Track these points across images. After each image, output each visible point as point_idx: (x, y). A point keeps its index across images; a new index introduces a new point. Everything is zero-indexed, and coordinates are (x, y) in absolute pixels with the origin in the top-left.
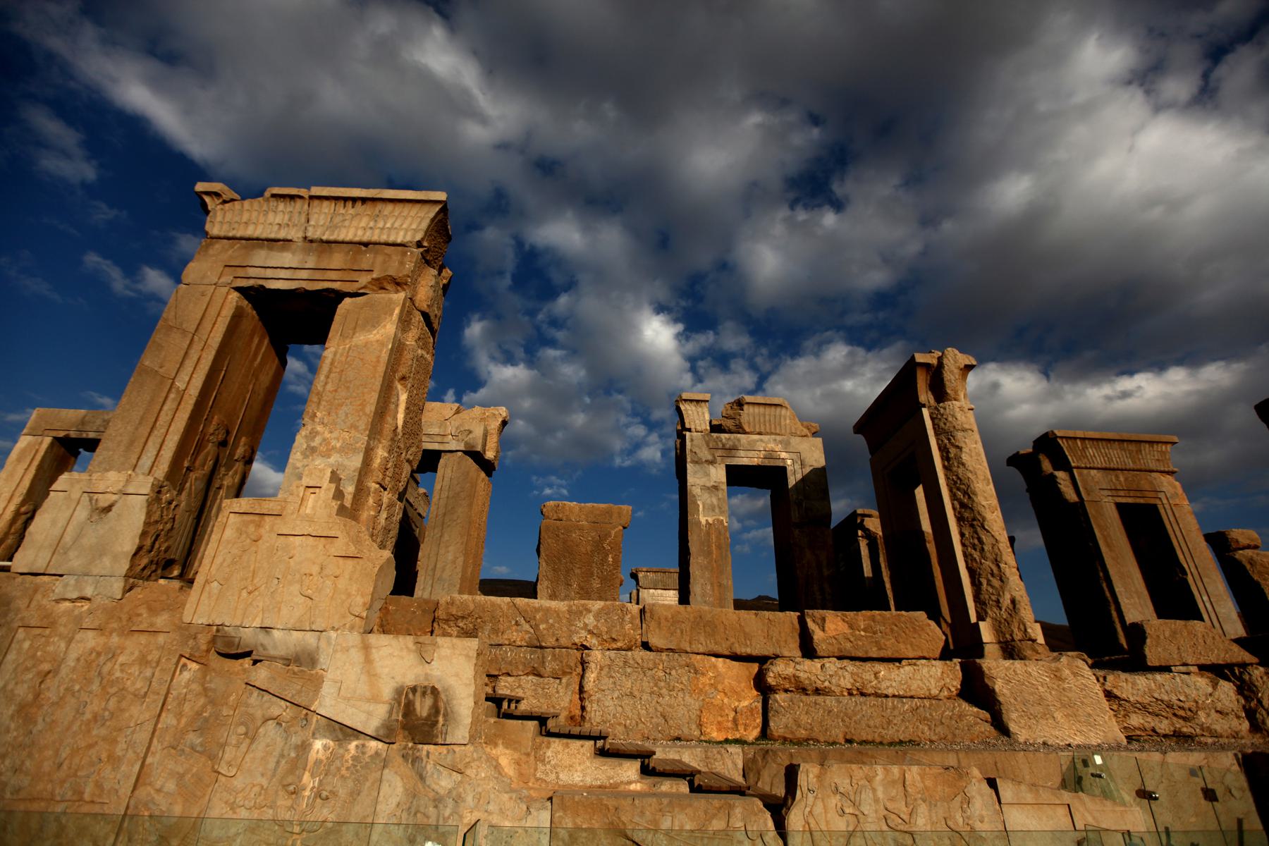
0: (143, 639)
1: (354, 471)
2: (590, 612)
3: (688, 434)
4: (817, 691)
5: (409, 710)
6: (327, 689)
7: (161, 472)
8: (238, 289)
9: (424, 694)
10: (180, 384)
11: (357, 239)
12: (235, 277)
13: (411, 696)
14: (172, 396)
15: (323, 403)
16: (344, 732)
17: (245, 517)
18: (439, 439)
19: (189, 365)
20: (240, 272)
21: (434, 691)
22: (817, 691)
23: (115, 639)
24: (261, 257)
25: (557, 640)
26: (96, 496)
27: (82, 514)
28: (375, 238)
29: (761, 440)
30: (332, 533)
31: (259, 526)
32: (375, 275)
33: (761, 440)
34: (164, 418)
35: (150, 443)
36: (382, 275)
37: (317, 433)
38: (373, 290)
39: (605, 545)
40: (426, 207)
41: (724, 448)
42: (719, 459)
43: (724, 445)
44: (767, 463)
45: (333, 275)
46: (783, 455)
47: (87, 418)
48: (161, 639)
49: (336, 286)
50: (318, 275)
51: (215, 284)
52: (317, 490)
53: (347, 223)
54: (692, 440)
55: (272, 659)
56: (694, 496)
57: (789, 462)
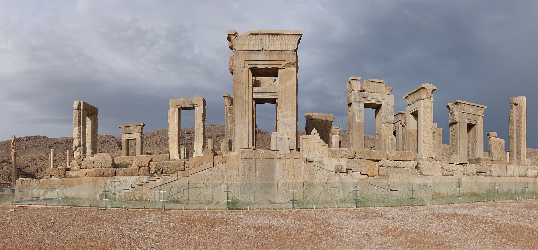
8: (250, 68)
20: (249, 63)
24: (253, 57)
45: (275, 62)
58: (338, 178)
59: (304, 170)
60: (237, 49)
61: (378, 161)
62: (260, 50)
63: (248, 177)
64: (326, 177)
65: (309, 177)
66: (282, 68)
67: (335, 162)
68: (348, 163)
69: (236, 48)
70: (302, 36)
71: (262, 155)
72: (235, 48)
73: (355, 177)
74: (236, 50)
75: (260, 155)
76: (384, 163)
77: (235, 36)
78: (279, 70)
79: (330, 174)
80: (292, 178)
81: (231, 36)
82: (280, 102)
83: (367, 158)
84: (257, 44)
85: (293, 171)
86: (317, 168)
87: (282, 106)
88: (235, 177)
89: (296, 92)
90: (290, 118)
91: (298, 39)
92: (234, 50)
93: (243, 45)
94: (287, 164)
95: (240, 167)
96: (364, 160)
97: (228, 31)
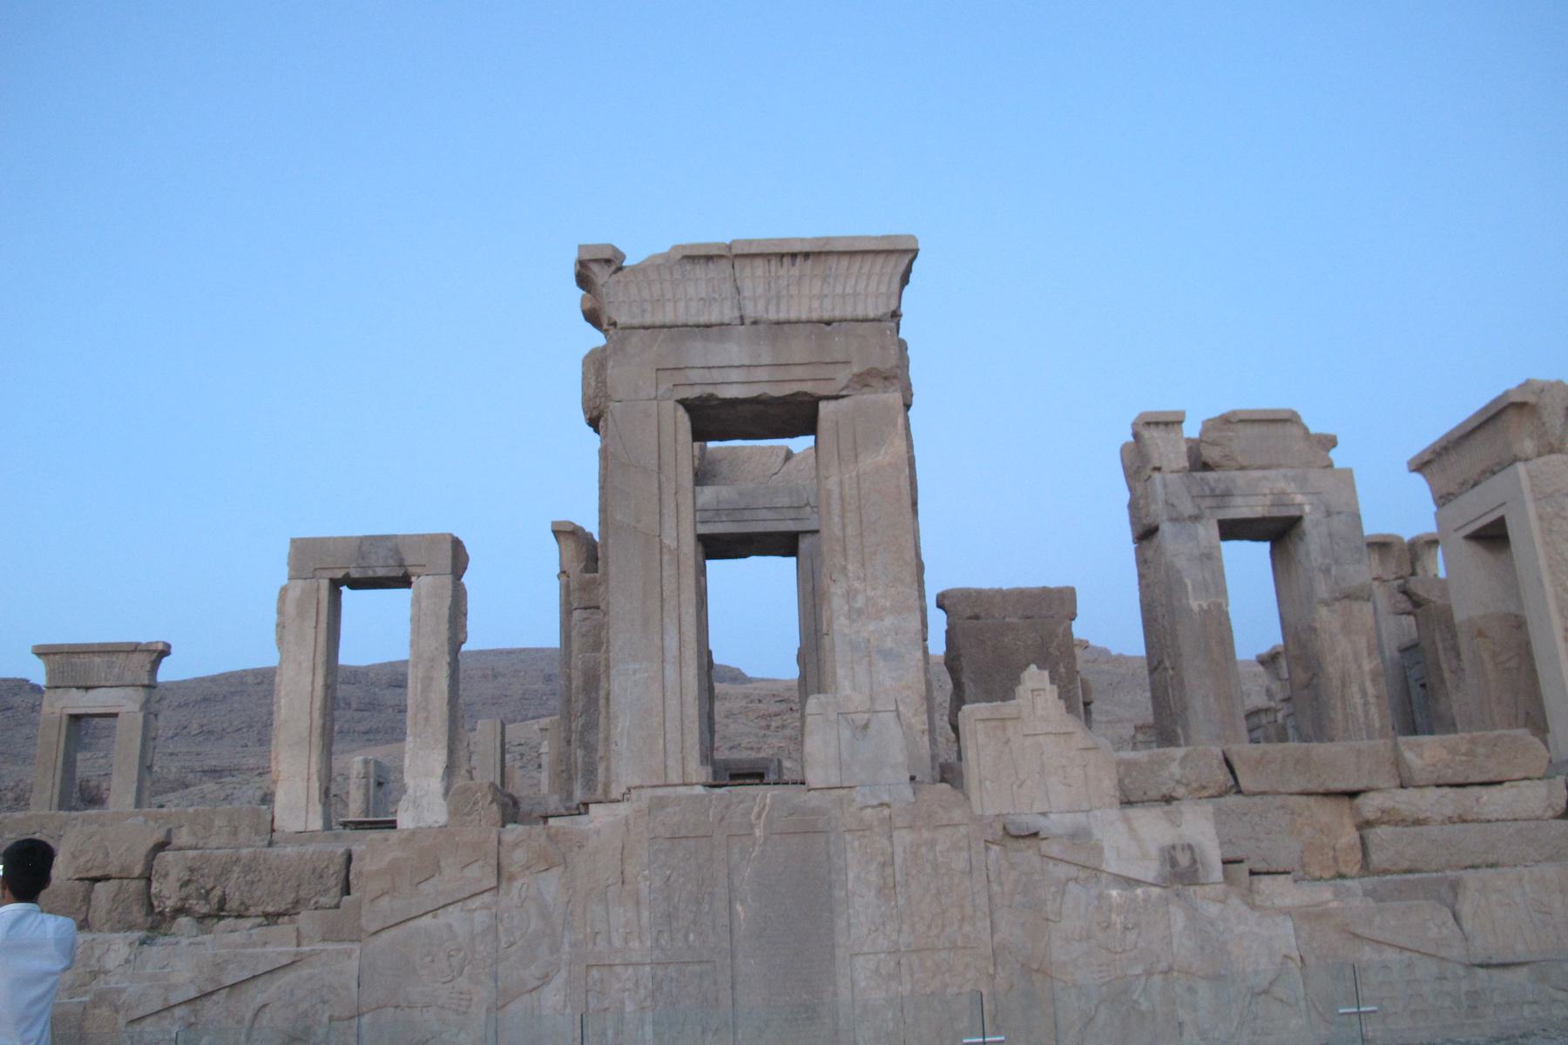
0: (948, 831)
1: (916, 634)
2: (1174, 760)
3: (1156, 475)
4: (1418, 822)
5: (1174, 863)
6: (1109, 854)
7: (692, 652)
8: (683, 402)
9: (1183, 849)
10: (669, 541)
11: (815, 316)
12: (674, 385)
13: (1172, 852)
14: (666, 558)
15: (850, 553)
16: (1130, 882)
17: (988, 723)
18: (792, 513)
19: (669, 511)
20: (679, 377)
21: (1190, 847)
22: (1418, 822)
23: (926, 834)
24: (697, 352)
25: (1145, 793)
26: (849, 717)
27: (846, 734)
28: (838, 314)
29: (1266, 478)
30: (1070, 729)
31: (1004, 729)
32: (856, 369)
33: (1266, 478)
34: (669, 588)
35: (667, 620)
36: (865, 369)
37: (857, 591)
38: (855, 389)
39: (1051, 650)
40: (893, 259)
41: (1213, 495)
42: (1208, 512)
43: (1212, 490)
44: (1276, 512)
45: (799, 372)
46: (1299, 498)
47: (364, 548)
48: (963, 830)
49: (808, 387)
50: (780, 374)
51: (655, 399)
52: (1041, 692)
53: (794, 290)
54: (1165, 486)
55: (1061, 837)
56: (1179, 572)
57: (1307, 508)
58: (1179, 919)
59: (995, 888)
60: (623, 319)
61: (1353, 795)
62: (727, 322)
63: (691, 937)
64: (1113, 916)
65: (1023, 925)
66: (834, 394)
67: (1153, 828)
68: (1221, 818)
69: (616, 318)
70: (917, 254)
71: (759, 816)
72: (609, 318)
73: (1268, 904)
74: (614, 324)
75: (753, 818)
76: (1389, 804)
77: (613, 268)
78: (823, 405)
79: (1136, 896)
80: (934, 932)
81: (595, 268)
82: (838, 548)
83: (1295, 788)
84: (716, 296)
85: (934, 892)
86: (1061, 871)
87: (850, 567)
88: (617, 942)
89: (912, 495)
90: (889, 621)
91: (902, 268)
92: (605, 327)
93: (647, 306)
94: (898, 861)
95: (644, 886)
96: (1279, 800)
97: (581, 247)
